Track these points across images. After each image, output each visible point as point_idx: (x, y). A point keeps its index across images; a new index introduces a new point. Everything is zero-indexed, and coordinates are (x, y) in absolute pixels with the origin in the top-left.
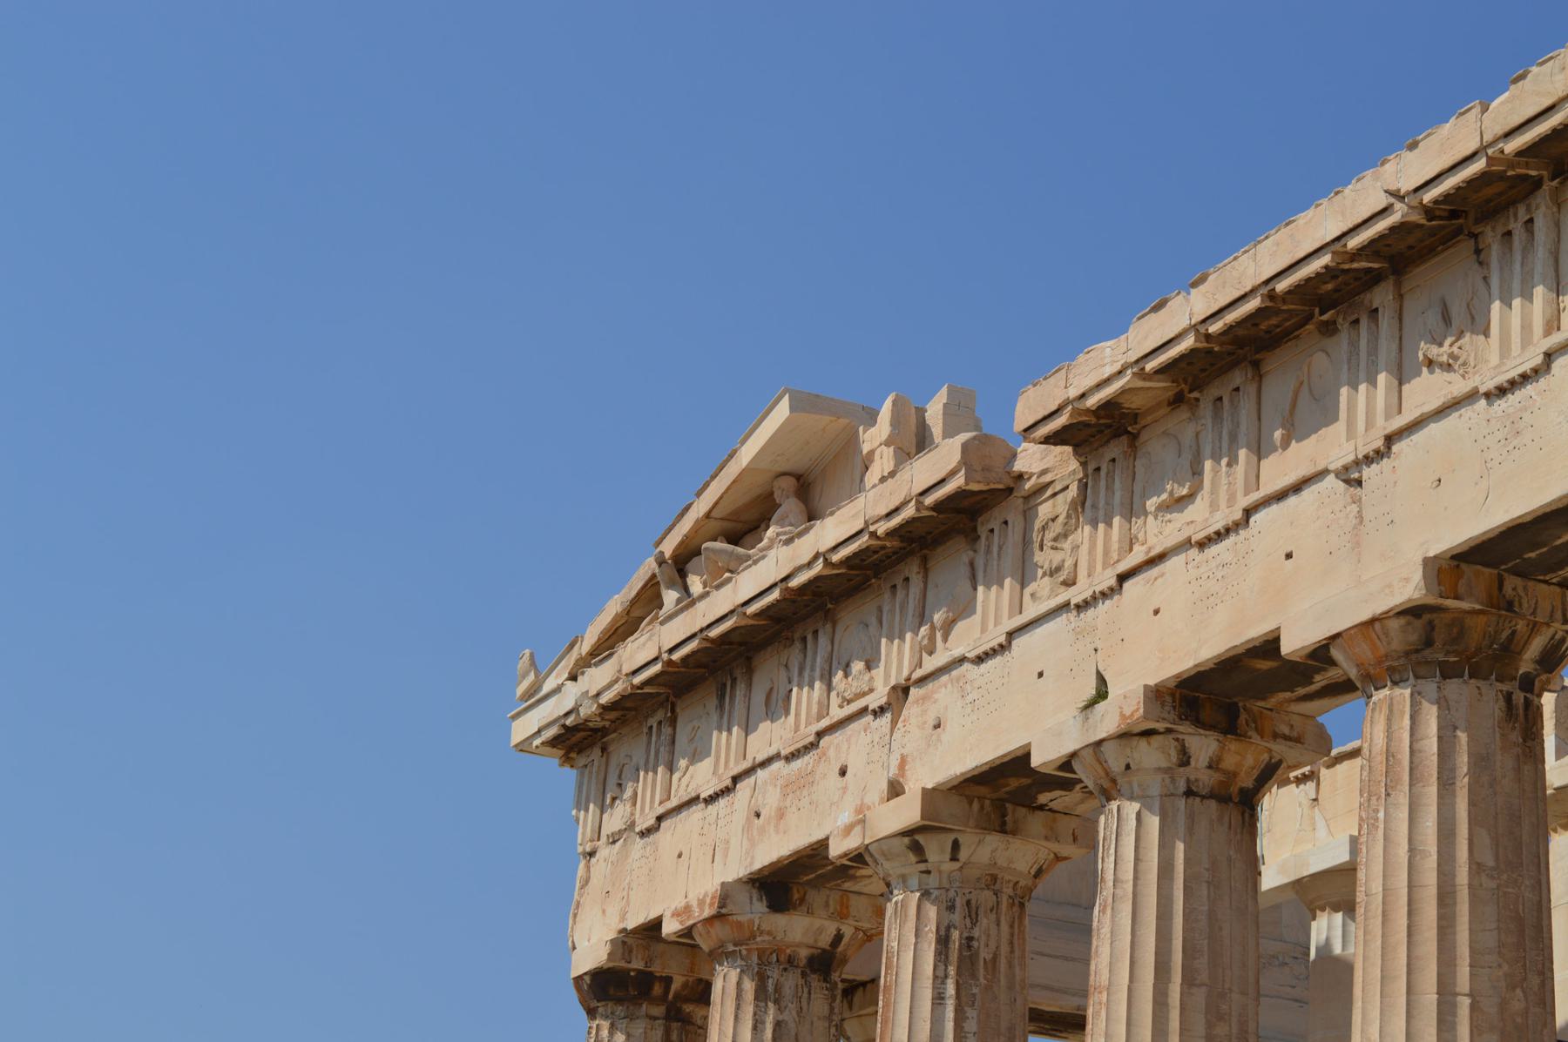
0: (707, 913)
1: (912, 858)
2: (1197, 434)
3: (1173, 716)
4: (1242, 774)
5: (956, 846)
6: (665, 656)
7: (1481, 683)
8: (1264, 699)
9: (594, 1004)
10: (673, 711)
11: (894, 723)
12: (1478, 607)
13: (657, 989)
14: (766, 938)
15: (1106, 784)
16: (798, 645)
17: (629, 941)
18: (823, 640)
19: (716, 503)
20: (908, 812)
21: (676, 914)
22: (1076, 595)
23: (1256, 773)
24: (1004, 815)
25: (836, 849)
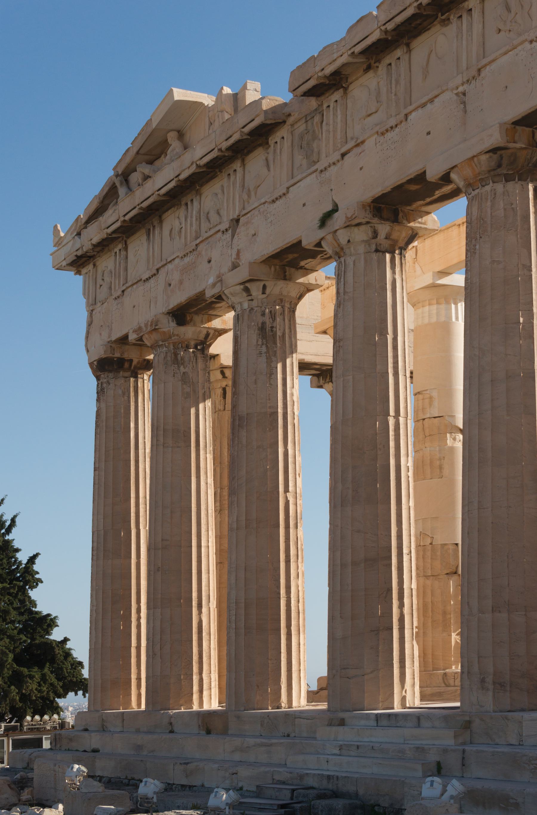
0: (149, 329)
1: (245, 294)
2: (378, 83)
3: (370, 216)
4: (400, 241)
5: (264, 287)
6: (122, 219)
7: (523, 183)
8: (410, 205)
9: (99, 373)
10: (126, 244)
11: (233, 236)
12: (524, 146)
13: (126, 365)
14: (176, 337)
15: (338, 250)
16: (183, 207)
17: (113, 345)
18: (196, 203)
19: (142, 147)
20: (243, 273)
21: (135, 331)
22: (320, 166)
23: (406, 240)
24: (285, 272)
25: (209, 293)
